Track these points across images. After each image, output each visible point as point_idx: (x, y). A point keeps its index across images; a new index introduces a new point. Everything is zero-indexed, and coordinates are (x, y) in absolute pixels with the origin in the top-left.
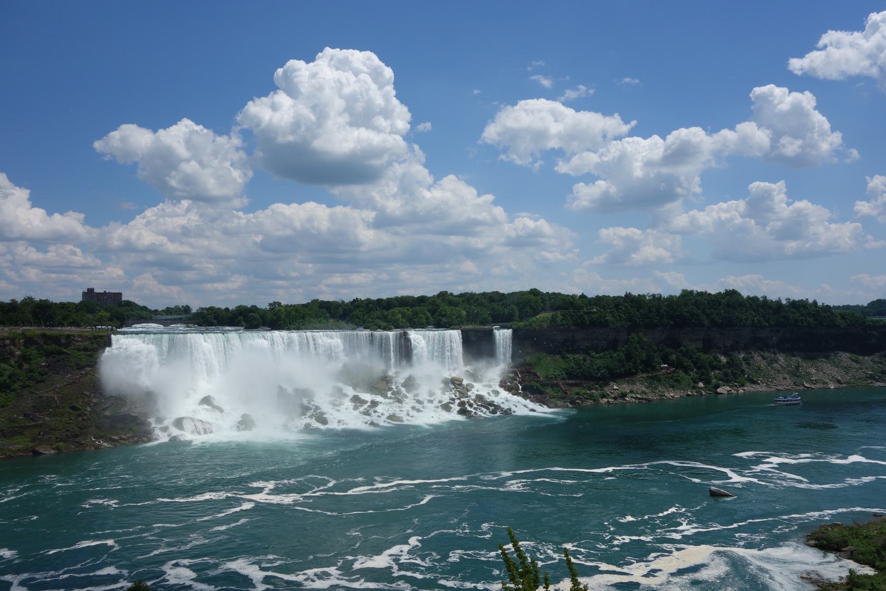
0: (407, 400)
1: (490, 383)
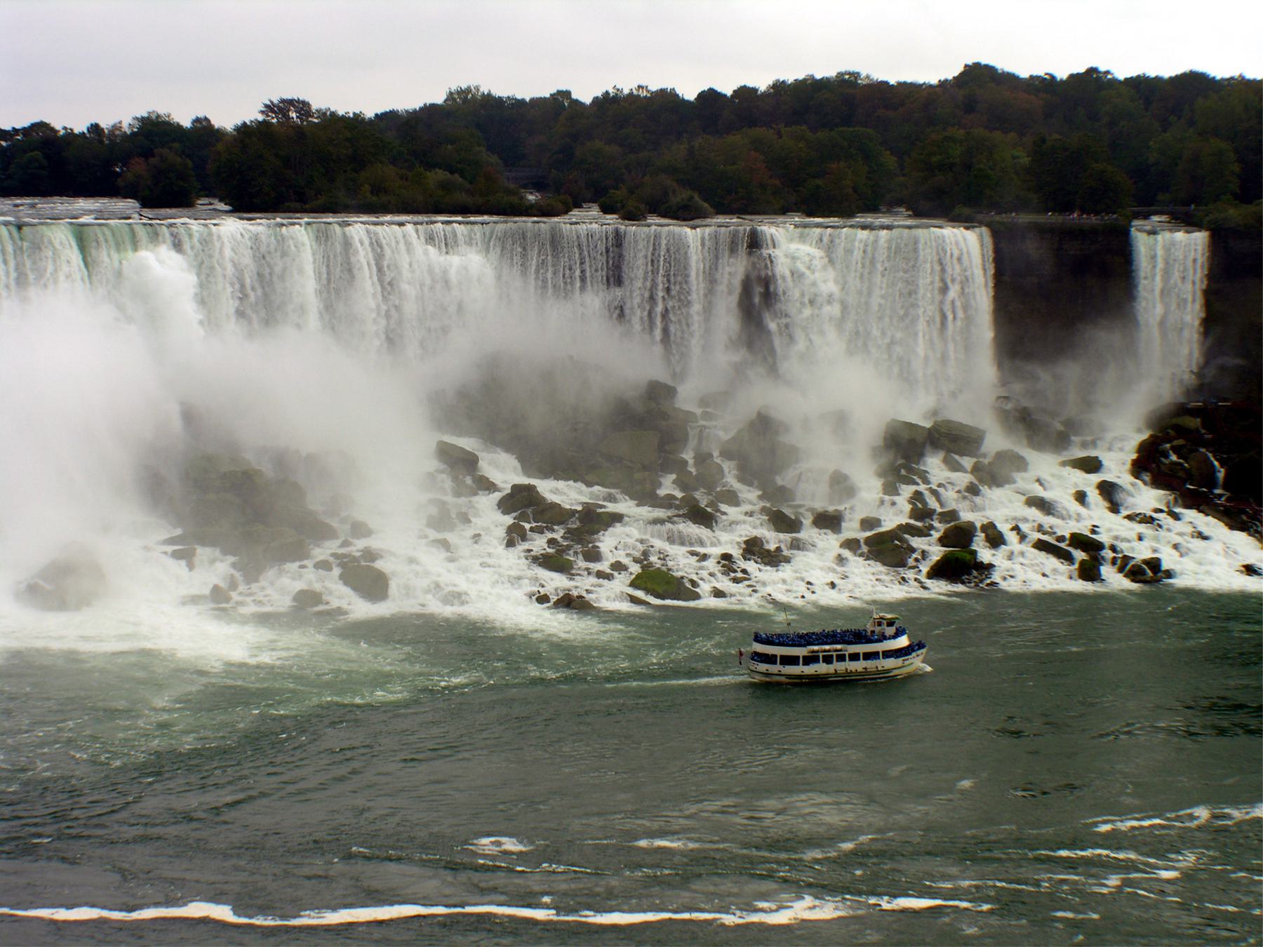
0: (732, 512)
1: (1093, 453)
